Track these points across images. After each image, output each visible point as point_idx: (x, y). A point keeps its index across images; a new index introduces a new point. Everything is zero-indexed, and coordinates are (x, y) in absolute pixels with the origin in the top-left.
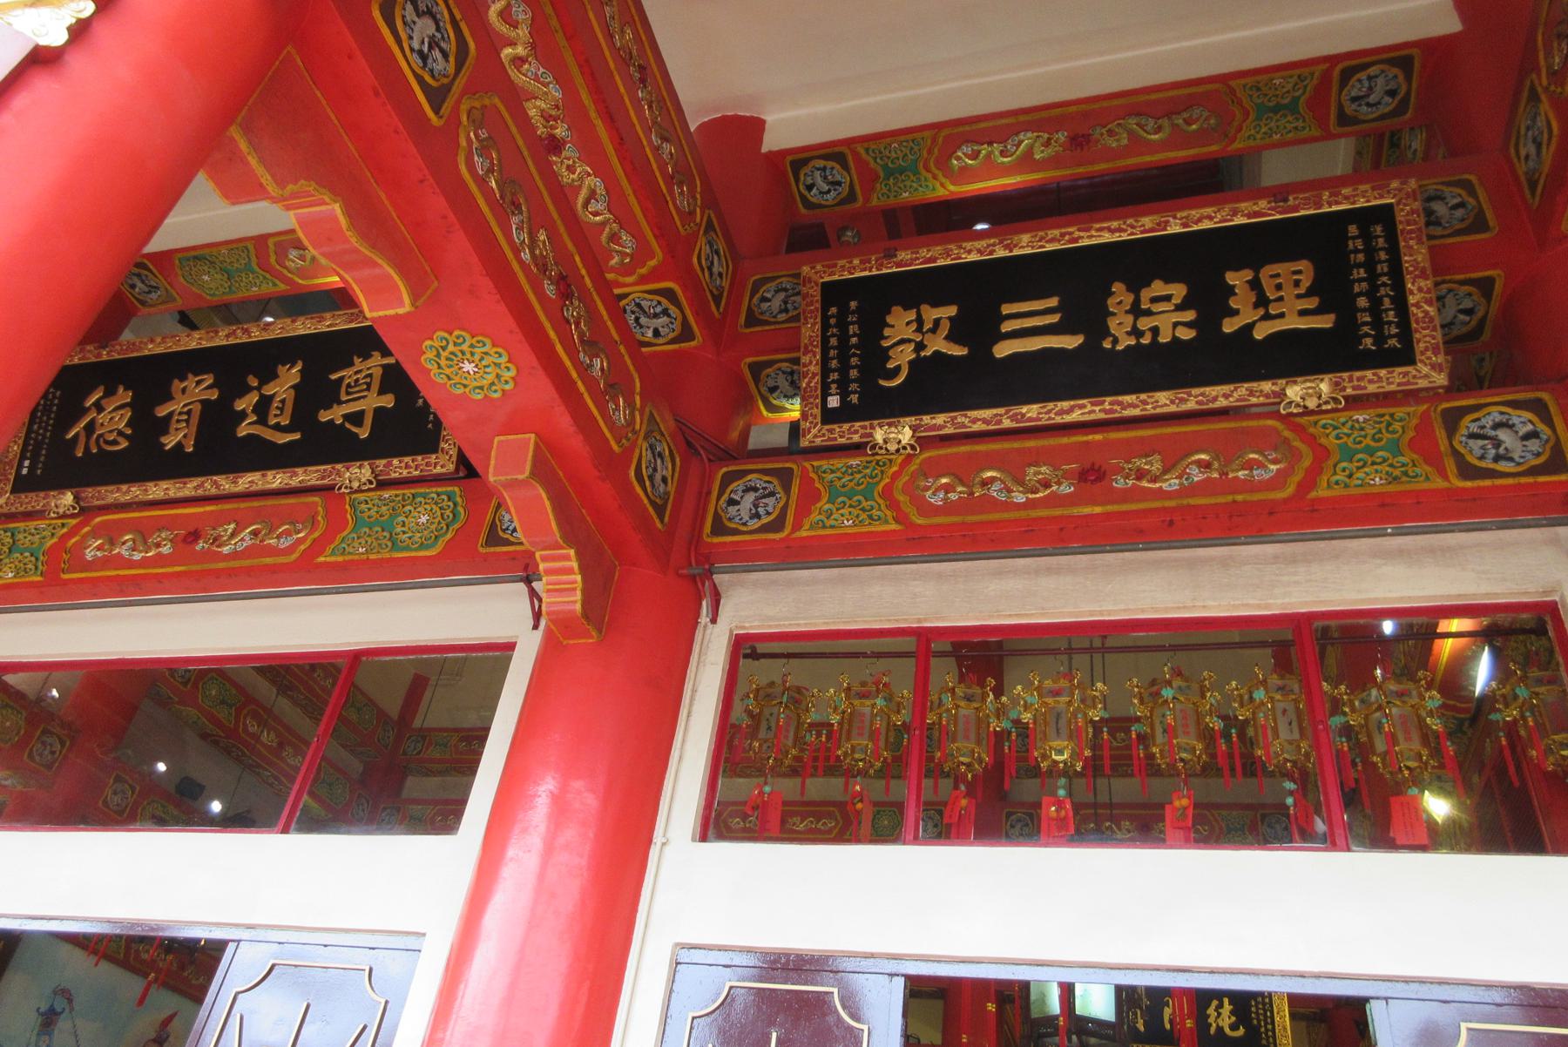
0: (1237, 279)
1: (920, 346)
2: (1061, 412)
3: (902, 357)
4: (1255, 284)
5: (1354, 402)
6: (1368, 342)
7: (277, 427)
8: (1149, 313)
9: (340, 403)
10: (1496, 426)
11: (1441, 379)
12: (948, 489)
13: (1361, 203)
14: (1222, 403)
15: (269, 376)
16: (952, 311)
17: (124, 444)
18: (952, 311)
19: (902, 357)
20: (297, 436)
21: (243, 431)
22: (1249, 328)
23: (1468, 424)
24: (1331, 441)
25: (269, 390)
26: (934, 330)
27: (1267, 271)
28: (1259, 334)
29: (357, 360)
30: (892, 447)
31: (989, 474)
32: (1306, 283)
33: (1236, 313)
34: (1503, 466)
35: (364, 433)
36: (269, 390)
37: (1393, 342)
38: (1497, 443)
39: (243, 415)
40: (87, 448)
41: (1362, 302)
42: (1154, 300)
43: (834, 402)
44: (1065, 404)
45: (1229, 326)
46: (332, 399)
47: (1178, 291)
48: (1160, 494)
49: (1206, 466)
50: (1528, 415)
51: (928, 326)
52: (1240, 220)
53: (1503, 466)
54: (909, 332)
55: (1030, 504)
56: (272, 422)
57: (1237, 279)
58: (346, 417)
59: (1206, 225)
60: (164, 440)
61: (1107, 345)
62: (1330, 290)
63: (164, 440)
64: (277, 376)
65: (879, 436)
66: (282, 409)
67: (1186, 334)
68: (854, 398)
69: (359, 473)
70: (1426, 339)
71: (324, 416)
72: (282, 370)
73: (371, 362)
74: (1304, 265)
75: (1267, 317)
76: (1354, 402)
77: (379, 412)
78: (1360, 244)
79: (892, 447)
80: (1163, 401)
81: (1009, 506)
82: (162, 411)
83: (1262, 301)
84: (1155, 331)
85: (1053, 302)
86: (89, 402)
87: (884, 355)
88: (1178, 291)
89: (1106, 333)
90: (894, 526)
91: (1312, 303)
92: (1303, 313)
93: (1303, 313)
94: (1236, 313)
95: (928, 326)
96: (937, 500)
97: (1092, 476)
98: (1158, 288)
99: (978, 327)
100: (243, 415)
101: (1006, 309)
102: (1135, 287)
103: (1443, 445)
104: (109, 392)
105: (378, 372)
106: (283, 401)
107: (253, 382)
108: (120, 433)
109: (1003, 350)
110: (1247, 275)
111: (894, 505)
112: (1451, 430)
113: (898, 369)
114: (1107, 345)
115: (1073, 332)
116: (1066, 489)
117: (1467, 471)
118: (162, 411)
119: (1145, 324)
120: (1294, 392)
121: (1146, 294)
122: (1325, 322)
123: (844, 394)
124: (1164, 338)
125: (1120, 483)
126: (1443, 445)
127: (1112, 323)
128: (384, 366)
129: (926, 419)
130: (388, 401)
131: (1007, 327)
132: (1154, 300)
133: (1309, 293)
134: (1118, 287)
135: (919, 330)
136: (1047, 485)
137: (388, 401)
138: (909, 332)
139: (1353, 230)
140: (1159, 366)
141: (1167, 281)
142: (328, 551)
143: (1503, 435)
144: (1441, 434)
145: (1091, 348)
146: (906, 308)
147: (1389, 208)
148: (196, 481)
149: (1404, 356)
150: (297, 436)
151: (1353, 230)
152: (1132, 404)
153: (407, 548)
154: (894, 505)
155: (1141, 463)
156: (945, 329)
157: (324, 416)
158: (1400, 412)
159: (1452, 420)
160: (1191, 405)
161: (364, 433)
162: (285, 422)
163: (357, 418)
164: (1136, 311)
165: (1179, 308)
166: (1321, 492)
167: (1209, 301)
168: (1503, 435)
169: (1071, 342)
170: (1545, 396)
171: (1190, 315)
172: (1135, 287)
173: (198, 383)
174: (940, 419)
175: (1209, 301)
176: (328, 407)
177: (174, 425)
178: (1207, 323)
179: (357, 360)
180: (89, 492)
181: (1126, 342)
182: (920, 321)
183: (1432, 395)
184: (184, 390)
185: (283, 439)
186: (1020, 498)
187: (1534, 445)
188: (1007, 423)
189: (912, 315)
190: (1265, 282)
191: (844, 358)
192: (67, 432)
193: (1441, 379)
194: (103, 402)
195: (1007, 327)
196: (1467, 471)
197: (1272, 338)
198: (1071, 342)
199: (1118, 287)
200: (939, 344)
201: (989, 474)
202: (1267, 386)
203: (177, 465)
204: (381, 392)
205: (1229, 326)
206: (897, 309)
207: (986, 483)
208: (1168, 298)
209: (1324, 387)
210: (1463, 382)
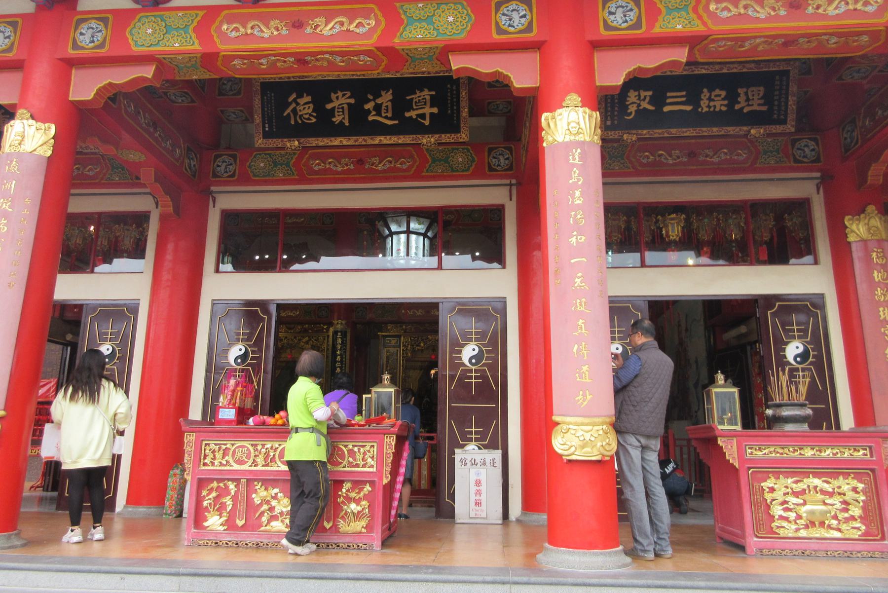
0: (741, 91)
1: (639, 105)
2: (683, 132)
3: (632, 109)
4: (746, 94)
5: (769, 135)
6: (775, 116)
7: (386, 117)
8: (713, 100)
9: (414, 110)
10: (806, 146)
11: (793, 130)
12: (648, 157)
13: (781, 68)
14: (732, 133)
15: (377, 95)
16: (650, 93)
17: (314, 120)
18: (650, 93)
19: (632, 109)
20: (397, 122)
21: (370, 118)
22: (742, 108)
23: (797, 145)
24: (760, 148)
25: (379, 101)
26: (644, 100)
27: (751, 89)
28: (745, 111)
29: (418, 92)
30: (629, 141)
31: (661, 152)
32: (761, 94)
33: (739, 103)
34: (805, 160)
35: (427, 123)
36: (379, 101)
37: (782, 117)
38: (804, 152)
39: (369, 112)
40: (296, 121)
41: (776, 103)
42: (716, 96)
43: (609, 123)
44: (684, 130)
45: (737, 107)
46: (410, 108)
47: (723, 93)
48: (713, 163)
49: (726, 154)
50: (813, 143)
51: (642, 97)
52: (744, 70)
53: (805, 160)
54: (635, 100)
55: (675, 164)
56: (384, 115)
57: (741, 91)
58: (417, 115)
59: (735, 71)
60: (334, 120)
61: (700, 110)
62: (768, 99)
63: (334, 120)
64: (381, 96)
65: (625, 137)
66: (387, 110)
67: (724, 109)
68: (616, 122)
69: (428, 140)
70: (792, 117)
71: (407, 115)
72: (383, 93)
73: (423, 93)
74: (762, 88)
75: (748, 105)
76: (769, 135)
77: (432, 114)
78: (779, 83)
79: (629, 141)
80: (715, 130)
81: (667, 164)
82: (329, 106)
83: (748, 100)
84: (715, 106)
85: (684, 93)
86: (290, 100)
87: (627, 107)
88: (723, 93)
89: (700, 106)
90: (632, 170)
91: (762, 101)
92: (759, 105)
93: (759, 105)
94: (739, 103)
95: (642, 97)
96: (645, 161)
97: (692, 155)
98: (717, 92)
99: (659, 100)
100: (369, 112)
101: (669, 94)
102: (711, 90)
103: (790, 152)
104: (300, 96)
105: (428, 98)
106: (387, 106)
107: (371, 97)
108: (310, 115)
109: (666, 109)
110: (745, 90)
111: (631, 162)
112: (793, 145)
113: (631, 113)
114: (700, 110)
115: (690, 105)
116: (685, 160)
117: (796, 161)
118: (329, 106)
119: (712, 104)
120: (753, 131)
121: (714, 94)
122: (764, 108)
123: (612, 120)
124: (717, 109)
125: (701, 158)
126: (790, 152)
127: (702, 103)
128: (431, 95)
129: (640, 131)
130: (435, 110)
131: (668, 101)
132: (716, 96)
133: (762, 98)
134: (705, 90)
135: (639, 99)
136: (678, 157)
137: (435, 110)
138: (635, 100)
139: (777, 77)
140: (714, 118)
141: (721, 89)
142: (425, 170)
143: (806, 149)
144: (790, 147)
145: (695, 110)
146: (635, 91)
147: (788, 71)
148: (354, 138)
149: (784, 122)
150: (397, 122)
151: (777, 77)
152: (705, 131)
153: (457, 171)
154: (631, 162)
155: (707, 151)
156: (648, 99)
157: (407, 115)
158: (780, 139)
159: (794, 142)
160: (722, 133)
161: (427, 123)
162: (390, 115)
163: (423, 116)
164: (710, 99)
165: (723, 99)
166: (758, 165)
167: (732, 98)
168: (806, 149)
169: (688, 108)
170: (818, 137)
171: (726, 102)
172: (711, 90)
173: (344, 95)
174: (645, 132)
175: (732, 98)
176: (409, 111)
177: (336, 114)
178: (730, 106)
179: (418, 92)
180: (302, 140)
181: (705, 109)
182: (639, 95)
183: (791, 134)
184: (337, 98)
185: (389, 122)
186: (671, 162)
187: (813, 153)
188: (666, 135)
189: (637, 93)
190: (750, 93)
191: (613, 107)
192: (284, 112)
193: (793, 130)
194: (298, 100)
195: (668, 101)
196: (796, 161)
197: (749, 112)
198: (688, 108)
199: (705, 90)
200: (645, 105)
201: (661, 152)
202: (745, 128)
203: (340, 130)
204: (432, 106)
205: (737, 107)
206: (632, 91)
207: (660, 155)
208: (720, 96)
209: (762, 131)
210: (799, 130)
